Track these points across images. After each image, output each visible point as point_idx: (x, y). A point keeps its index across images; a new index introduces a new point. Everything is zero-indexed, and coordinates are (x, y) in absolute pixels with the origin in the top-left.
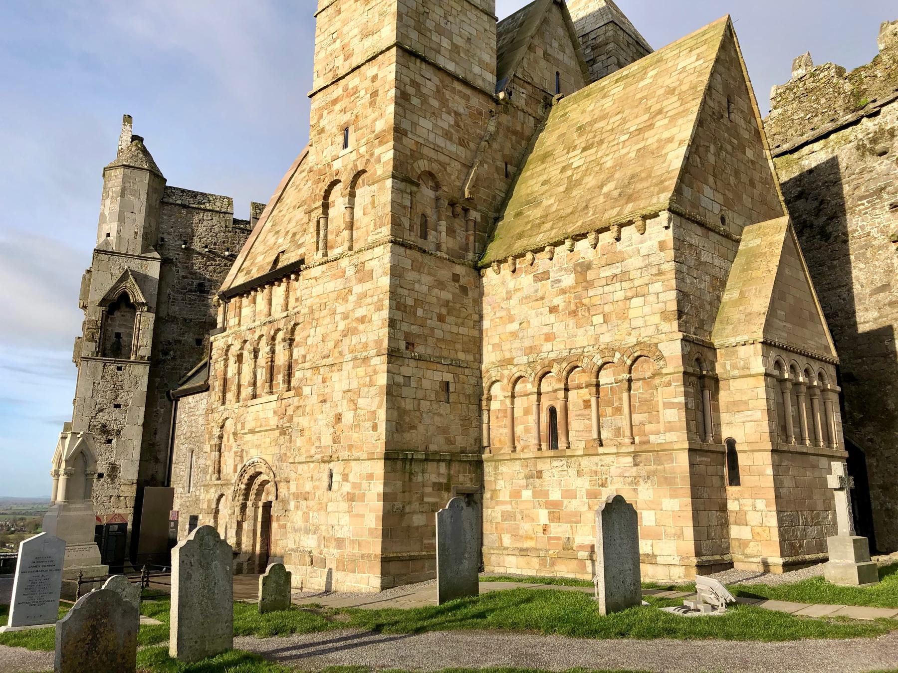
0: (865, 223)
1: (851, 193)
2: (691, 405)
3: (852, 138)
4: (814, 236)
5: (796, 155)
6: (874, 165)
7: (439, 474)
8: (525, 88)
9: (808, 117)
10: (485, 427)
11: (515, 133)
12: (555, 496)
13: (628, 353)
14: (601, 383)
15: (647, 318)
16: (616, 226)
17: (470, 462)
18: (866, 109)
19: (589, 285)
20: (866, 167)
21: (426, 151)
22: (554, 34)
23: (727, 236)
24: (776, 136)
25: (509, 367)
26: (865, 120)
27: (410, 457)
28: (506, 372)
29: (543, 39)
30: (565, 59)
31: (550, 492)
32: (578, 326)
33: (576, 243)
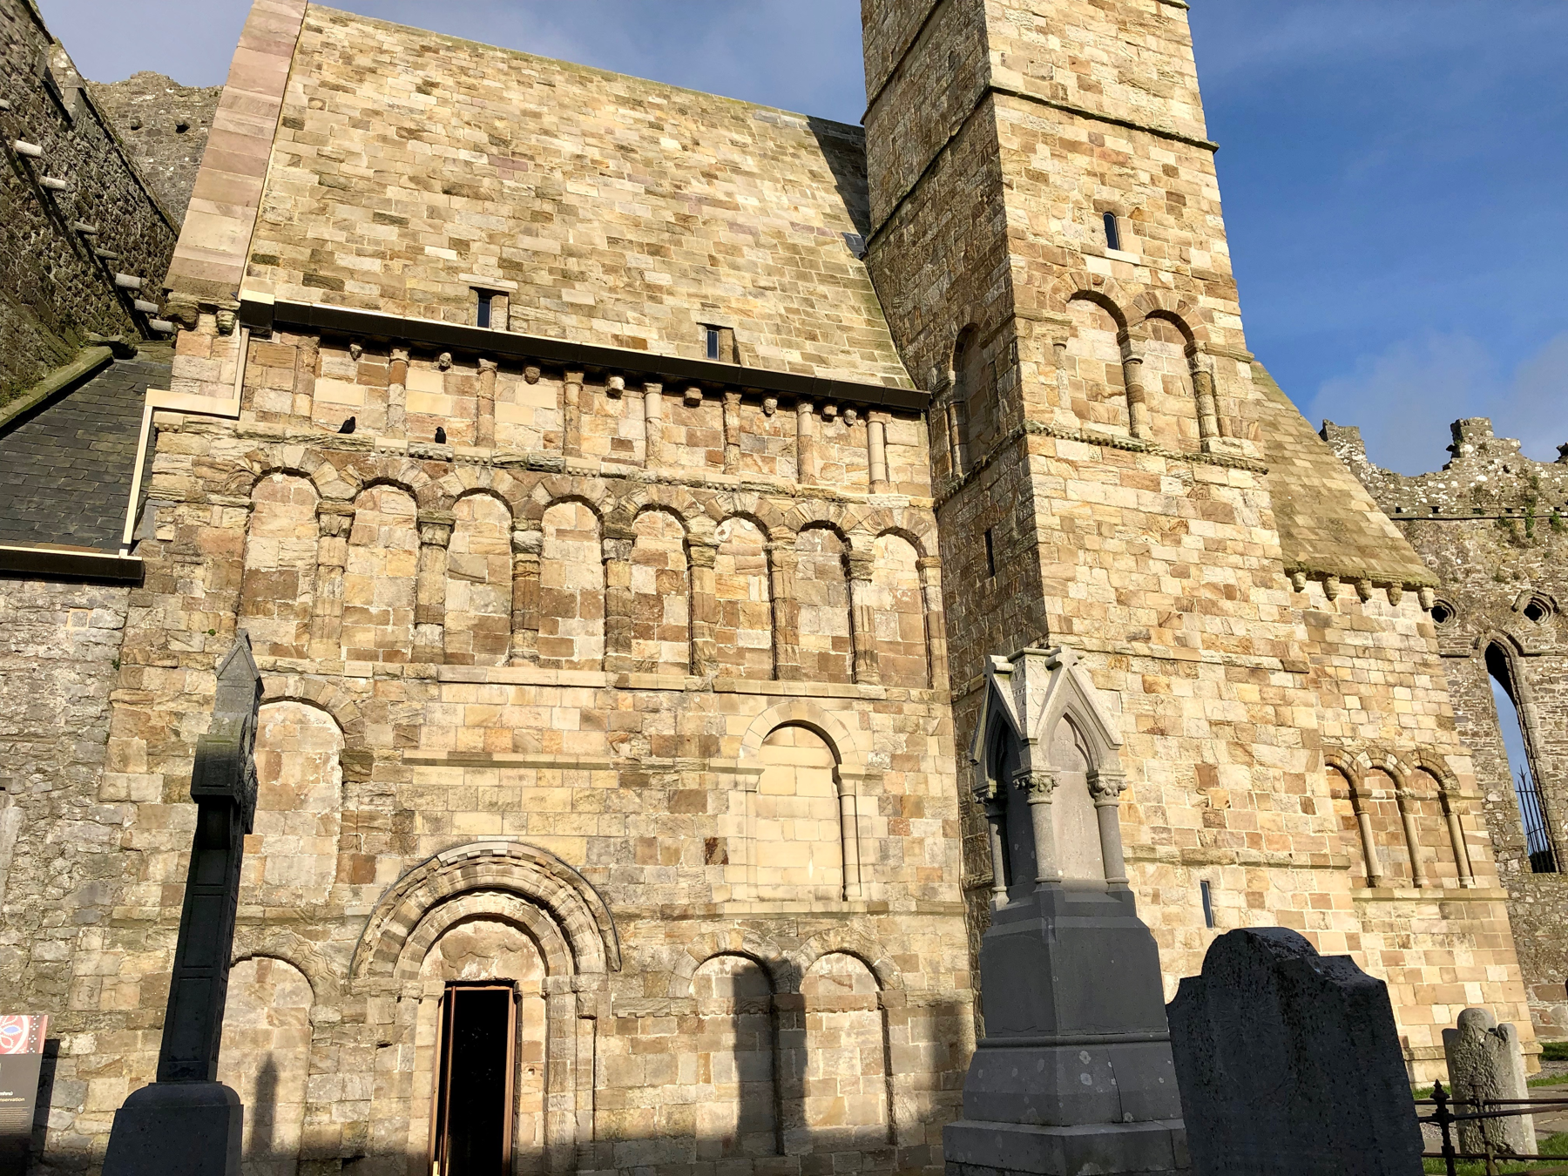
19: (1332, 649)
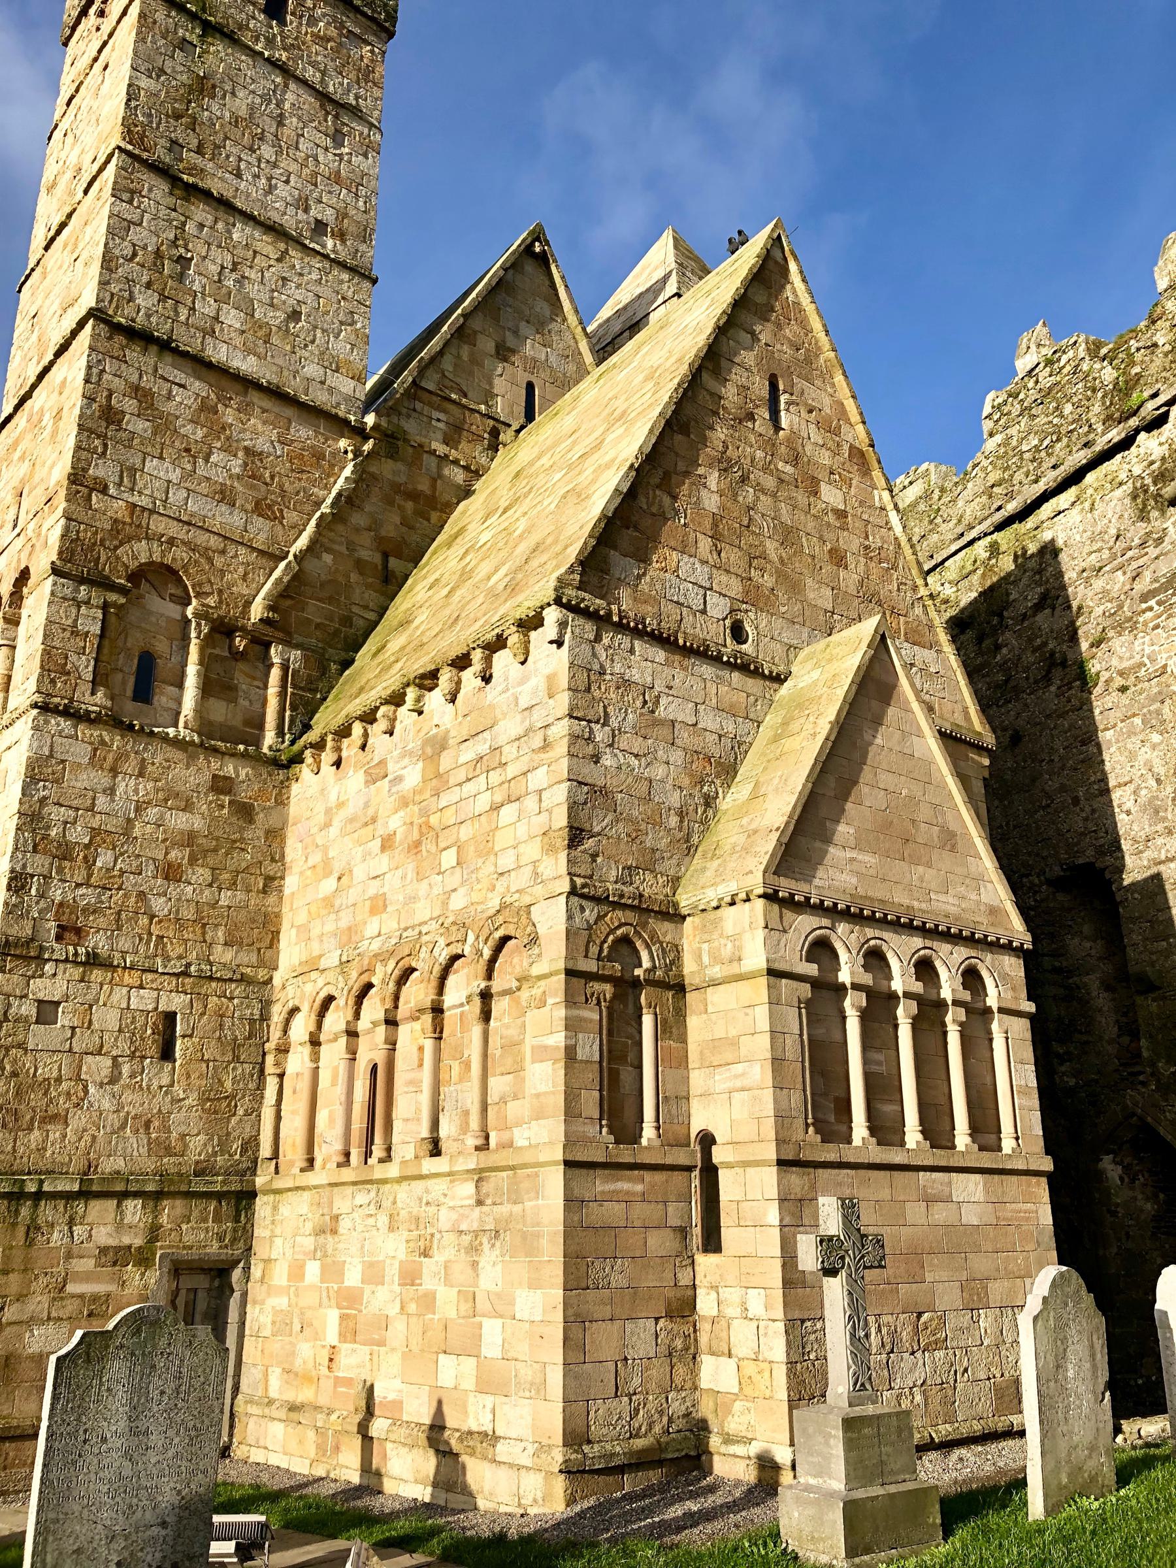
0: (1156, 648)
1: (1128, 587)
2: (590, 1048)
3: (1123, 476)
4: (1070, 683)
5: (1031, 522)
6: (1165, 526)
7: (120, 1226)
8: (445, 411)
9: (1046, 443)
10: (268, 1114)
11: (414, 496)
12: (353, 1277)
13: (485, 932)
14: (445, 1007)
15: (522, 848)
16: (479, 651)
17: (219, 1196)
18: (1143, 412)
20: (1151, 532)
21: (158, 525)
22: (527, 312)
23: (748, 668)
24: (995, 489)
25: (314, 975)
26: (1143, 436)
27: (32, 1188)
28: (309, 988)
29: (497, 319)
30: (552, 359)
31: (347, 1266)
32: (420, 876)
33: (428, 695)
